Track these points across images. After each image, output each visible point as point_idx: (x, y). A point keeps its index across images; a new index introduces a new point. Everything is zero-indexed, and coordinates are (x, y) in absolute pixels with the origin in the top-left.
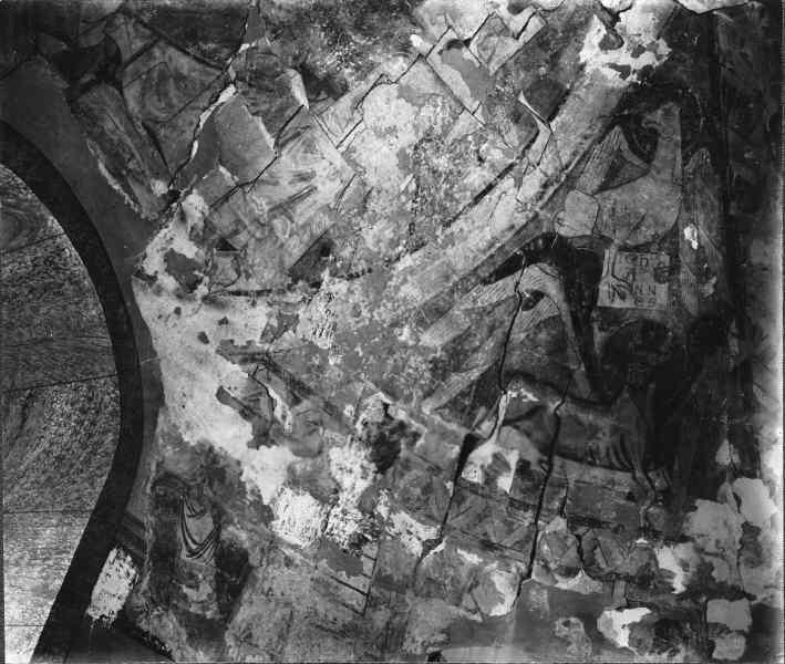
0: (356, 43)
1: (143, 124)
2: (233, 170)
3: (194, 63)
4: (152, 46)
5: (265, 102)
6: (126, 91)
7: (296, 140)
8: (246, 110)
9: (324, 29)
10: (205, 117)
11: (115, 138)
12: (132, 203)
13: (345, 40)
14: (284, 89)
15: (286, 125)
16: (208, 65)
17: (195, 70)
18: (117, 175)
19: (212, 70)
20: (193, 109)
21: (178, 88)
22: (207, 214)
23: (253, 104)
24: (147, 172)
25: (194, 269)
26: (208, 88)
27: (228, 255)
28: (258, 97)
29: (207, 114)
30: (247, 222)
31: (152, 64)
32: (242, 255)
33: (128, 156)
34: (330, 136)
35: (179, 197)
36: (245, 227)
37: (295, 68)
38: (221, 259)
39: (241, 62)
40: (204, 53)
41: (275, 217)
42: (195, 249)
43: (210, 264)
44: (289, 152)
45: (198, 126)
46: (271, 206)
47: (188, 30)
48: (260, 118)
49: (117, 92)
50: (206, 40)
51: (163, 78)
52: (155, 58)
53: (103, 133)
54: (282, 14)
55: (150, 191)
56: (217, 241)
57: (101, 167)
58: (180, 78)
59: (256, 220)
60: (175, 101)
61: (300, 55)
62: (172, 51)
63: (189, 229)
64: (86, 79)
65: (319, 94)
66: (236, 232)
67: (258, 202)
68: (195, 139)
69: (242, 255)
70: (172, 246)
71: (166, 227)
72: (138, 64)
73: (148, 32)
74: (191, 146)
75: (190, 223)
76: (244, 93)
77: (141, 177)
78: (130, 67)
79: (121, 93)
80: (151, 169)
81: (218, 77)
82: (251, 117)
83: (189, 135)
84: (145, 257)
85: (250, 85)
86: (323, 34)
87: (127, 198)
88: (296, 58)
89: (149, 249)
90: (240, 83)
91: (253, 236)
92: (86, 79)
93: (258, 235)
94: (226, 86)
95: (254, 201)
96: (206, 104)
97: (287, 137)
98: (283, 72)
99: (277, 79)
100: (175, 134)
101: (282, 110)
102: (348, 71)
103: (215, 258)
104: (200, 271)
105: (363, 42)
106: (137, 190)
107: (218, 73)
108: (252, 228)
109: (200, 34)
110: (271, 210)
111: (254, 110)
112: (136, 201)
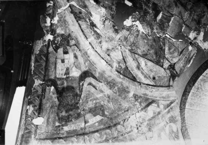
0: (145, 7)
1: (180, 56)
2: (182, 27)
3: (166, 46)
4: (166, 58)
5: (166, 24)
6: (175, 62)
7: (169, 11)
8: (169, 29)
9: (147, 17)
10: (174, 40)
11: (184, 63)
12: (194, 56)
13: (145, 10)
14: (161, 20)
15: (167, 16)
16: (165, 42)
17: (167, 46)
18: (190, 61)
19: (165, 41)
20: (174, 44)
21: (171, 49)
22: (193, 31)
23: (167, 28)
24: (188, 52)
25: (206, 31)
26: (168, 41)
27: (201, 20)
28: (165, 27)
29: (173, 39)
30: (192, 17)
31: (169, 57)
32: (200, 16)
33: (186, 58)
34: (164, 2)
35: (191, 42)
36: (193, 17)
37: (156, 20)
38: (202, 22)
39: (161, 34)
40: (163, 45)
41: (188, 9)
42: (201, 32)
43: (204, 26)
44: (172, 12)
45: (176, 41)
46: (186, 11)
47: (161, 50)
48: (169, 24)
49: (176, 64)
50: (161, 45)
51: (171, 53)
52: (168, 57)
53: (183, 66)
54: (149, 29)
55: (191, 51)
56: (198, 25)
57: (189, 66)
58: (169, 49)
59: (190, 15)
60: (174, 49)
61: (154, 20)
62: (166, 53)
63: (198, 36)
64: (175, 72)
65: (158, 10)
66: (195, 20)
67: (186, 16)
68: (179, 41)
69: (200, 16)
70: (202, 40)
71: (198, 43)
72: (170, 60)
73: (164, 60)
74: (180, 41)
75: (196, 36)
76: (166, 31)
77: (189, 54)
78: (171, 62)
79: (176, 63)
80: (187, 51)
81: (166, 39)
82: (170, 27)
83: (178, 43)
84: (205, 49)
85: (164, 30)
86: (148, 16)
87: (194, 57)
88: (155, 21)
89: (203, 48)
90: (165, 33)
91: (194, 14)
92: (175, 72)
93: (193, 12)
94: (166, 37)
95: (186, 18)
96: (171, 40)
97: (170, 14)
98: (158, 23)
99: (160, 24)
100: (180, 46)
101: (165, 19)
102: (150, 5)
103: (202, 25)
104: (206, 29)
105: (143, 5)
106: (192, 55)
107: (165, 39)
108: (192, 15)
109: (161, 47)
110: (187, 11)
111: (168, 26)
112: (194, 55)
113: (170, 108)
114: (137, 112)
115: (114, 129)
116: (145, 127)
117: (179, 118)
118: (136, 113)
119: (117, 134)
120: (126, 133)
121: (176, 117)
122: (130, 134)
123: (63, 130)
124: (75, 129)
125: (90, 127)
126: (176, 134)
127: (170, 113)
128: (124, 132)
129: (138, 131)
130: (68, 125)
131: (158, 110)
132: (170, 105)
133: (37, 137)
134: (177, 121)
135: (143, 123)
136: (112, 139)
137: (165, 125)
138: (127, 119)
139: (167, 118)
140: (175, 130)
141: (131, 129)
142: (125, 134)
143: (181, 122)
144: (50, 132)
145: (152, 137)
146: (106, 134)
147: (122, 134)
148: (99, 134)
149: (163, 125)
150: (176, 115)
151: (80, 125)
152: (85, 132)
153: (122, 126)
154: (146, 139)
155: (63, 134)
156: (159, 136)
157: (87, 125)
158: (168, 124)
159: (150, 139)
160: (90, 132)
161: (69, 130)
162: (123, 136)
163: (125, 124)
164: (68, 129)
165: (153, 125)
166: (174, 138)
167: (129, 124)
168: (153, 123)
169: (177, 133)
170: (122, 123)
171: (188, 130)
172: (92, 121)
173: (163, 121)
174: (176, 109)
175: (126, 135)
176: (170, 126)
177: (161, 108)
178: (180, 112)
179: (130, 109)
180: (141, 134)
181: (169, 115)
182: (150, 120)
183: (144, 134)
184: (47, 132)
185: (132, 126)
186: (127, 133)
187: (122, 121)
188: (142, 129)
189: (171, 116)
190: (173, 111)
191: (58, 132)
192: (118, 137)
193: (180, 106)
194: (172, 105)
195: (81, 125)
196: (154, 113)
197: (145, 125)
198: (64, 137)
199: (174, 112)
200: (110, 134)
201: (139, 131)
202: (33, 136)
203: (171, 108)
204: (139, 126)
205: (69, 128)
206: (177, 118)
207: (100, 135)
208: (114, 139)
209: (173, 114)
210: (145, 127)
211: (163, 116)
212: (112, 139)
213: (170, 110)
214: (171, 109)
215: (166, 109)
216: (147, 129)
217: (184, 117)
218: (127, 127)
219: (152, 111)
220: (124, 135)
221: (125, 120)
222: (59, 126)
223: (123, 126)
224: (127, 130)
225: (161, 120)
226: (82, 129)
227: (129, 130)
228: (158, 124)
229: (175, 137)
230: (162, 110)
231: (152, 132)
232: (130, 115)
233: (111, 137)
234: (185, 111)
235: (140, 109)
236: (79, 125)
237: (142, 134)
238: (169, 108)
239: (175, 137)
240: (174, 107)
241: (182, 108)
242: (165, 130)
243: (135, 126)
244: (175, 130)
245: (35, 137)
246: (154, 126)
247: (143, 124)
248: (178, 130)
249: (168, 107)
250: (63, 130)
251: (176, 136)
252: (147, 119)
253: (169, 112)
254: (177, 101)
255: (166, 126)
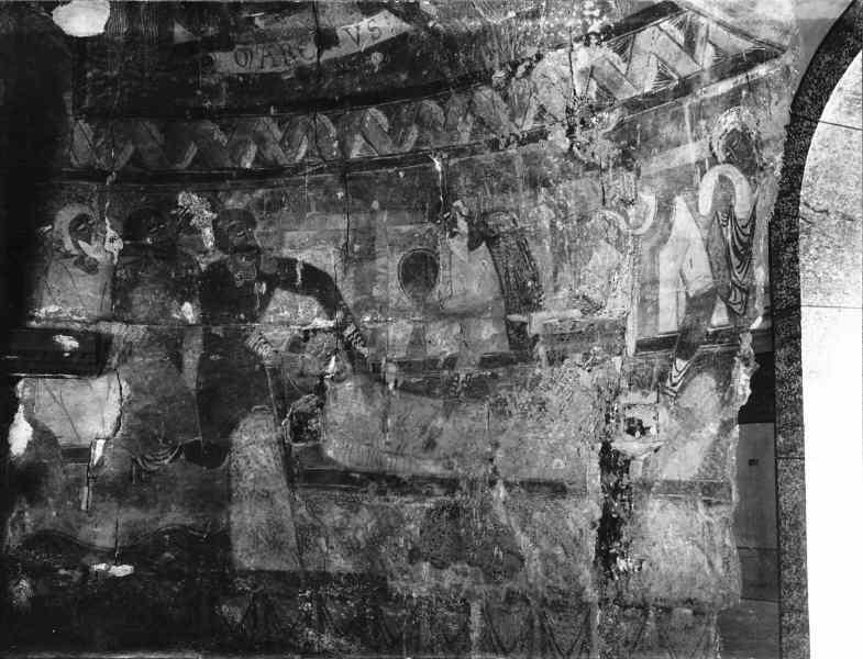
113: (744, 82)
114: (581, 39)
115: (457, 102)
116: (607, 136)
117: (775, 158)
118: (576, 46)
119: (474, 134)
120: (512, 138)
121: (762, 145)
122: (532, 147)
123: (214, 72)
124: (268, 69)
125: (344, 72)
126: (742, 237)
127: (742, 108)
128: (506, 133)
129: (572, 146)
130: (238, 46)
131: (684, 68)
132: (750, 66)
133: (87, 103)
134: (762, 169)
135: (599, 109)
136: (445, 156)
137: (700, 163)
138: (527, 63)
139: (717, 132)
140: (741, 211)
141: (538, 125)
142: (508, 143)
143: (781, 184)
144: (147, 75)
145: (632, 203)
146: (419, 121)
147: (494, 136)
148: (388, 115)
149: (693, 159)
150: (763, 137)
151: (295, 52)
152: (321, 95)
153: (498, 98)
154: (604, 201)
155: (213, 92)
156: (665, 209)
157: (327, 55)
158: (718, 163)
159: (622, 208)
160: (344, 99)
161: (242, 70)
162: (499, 150)
163: (516, 88)
164: (236, 66)
165: (645, 140)
166: (728, 249)
167: (534, 94)
168: (649, 128)
169: (748, 231)
170: (500, 74)
171: (803, 243)
172: (355, 35)
173: (695, 140)
174: (773, 102)
175: (512, 151)
176: (722, 178)
177: (700, 60)
178: (786, 127)
179: (547, 10)
180: (581, 168)
181: (729, 121)
182: (633, 105)
183: (596, 172)
184: (136, 78)
185: (549, 109)
186: (517, 137)
187: (502, 66)
188: (591, 139)
189: (739, 129)
190: (757, 104)
191: (191, 81)
192: (474, 153)
193: (796, 98)
194: (761, 70)
195: (301, 51)
196: (663, 77)
197: (610, 129)
198: (220, 111)
199: (762, 114)
200: (439, 129)
201: (575, 148)
202: (68, 97)
203: (752, 86)
204: (577, 120)
205: (243, 62)
206: (766, 153)
207: (392, 124)
208: (457, 156)
209: (751, 125)
210: (607, 136)
211: (700, 112)
212: (445, 156)
213: (744, 93)
214: (750, 90)
215: (722, 78)
216: (616, 152)
217: (801, 169)
218: (524, 109)
219: (653, 60)
220: (501, 147)
221: (515, 66)
222: (190, 47)
223: (506, 98)
224: (519, 121)
225: (688, 127)
226: (302, 73)
227: (529, 125)
228: (668, 142)
229: (735, 247)
230: (706, 77)
231: (632, 175)
232: (542, 44)
233: (444, 143)
234: (811, 135)
235: (595, 27)
236: (291, 54)
237: (589, 167)
238: (741, 79)
239: (735, 247)
240: (768, 86)
241: (803, 109)
242: (697, 189)
243: (562, 116)
244: (741, 211)
245: (77, 106)
246: (650, 149)
247: (599, 115)
248: (753, 217)
249: (734, 73)
250: (214, 72)
251: (740, 248)
252: (622, 96)
253: (733, 100)
254: (787, 59)
255: (703, 173)
